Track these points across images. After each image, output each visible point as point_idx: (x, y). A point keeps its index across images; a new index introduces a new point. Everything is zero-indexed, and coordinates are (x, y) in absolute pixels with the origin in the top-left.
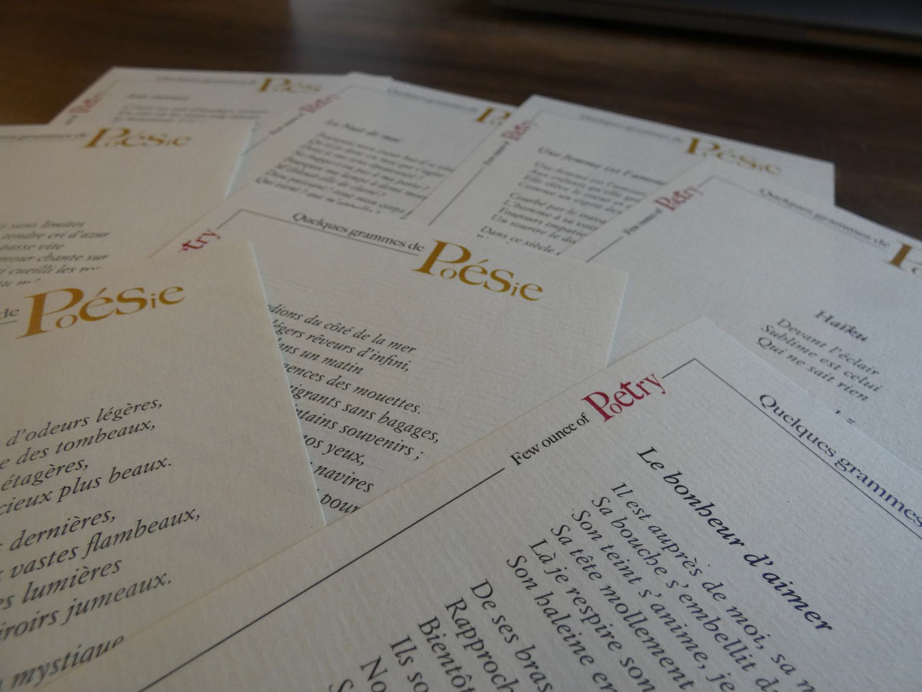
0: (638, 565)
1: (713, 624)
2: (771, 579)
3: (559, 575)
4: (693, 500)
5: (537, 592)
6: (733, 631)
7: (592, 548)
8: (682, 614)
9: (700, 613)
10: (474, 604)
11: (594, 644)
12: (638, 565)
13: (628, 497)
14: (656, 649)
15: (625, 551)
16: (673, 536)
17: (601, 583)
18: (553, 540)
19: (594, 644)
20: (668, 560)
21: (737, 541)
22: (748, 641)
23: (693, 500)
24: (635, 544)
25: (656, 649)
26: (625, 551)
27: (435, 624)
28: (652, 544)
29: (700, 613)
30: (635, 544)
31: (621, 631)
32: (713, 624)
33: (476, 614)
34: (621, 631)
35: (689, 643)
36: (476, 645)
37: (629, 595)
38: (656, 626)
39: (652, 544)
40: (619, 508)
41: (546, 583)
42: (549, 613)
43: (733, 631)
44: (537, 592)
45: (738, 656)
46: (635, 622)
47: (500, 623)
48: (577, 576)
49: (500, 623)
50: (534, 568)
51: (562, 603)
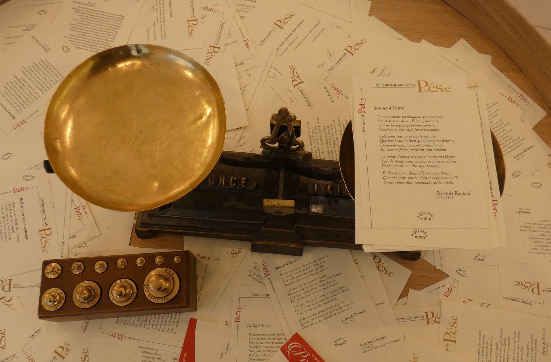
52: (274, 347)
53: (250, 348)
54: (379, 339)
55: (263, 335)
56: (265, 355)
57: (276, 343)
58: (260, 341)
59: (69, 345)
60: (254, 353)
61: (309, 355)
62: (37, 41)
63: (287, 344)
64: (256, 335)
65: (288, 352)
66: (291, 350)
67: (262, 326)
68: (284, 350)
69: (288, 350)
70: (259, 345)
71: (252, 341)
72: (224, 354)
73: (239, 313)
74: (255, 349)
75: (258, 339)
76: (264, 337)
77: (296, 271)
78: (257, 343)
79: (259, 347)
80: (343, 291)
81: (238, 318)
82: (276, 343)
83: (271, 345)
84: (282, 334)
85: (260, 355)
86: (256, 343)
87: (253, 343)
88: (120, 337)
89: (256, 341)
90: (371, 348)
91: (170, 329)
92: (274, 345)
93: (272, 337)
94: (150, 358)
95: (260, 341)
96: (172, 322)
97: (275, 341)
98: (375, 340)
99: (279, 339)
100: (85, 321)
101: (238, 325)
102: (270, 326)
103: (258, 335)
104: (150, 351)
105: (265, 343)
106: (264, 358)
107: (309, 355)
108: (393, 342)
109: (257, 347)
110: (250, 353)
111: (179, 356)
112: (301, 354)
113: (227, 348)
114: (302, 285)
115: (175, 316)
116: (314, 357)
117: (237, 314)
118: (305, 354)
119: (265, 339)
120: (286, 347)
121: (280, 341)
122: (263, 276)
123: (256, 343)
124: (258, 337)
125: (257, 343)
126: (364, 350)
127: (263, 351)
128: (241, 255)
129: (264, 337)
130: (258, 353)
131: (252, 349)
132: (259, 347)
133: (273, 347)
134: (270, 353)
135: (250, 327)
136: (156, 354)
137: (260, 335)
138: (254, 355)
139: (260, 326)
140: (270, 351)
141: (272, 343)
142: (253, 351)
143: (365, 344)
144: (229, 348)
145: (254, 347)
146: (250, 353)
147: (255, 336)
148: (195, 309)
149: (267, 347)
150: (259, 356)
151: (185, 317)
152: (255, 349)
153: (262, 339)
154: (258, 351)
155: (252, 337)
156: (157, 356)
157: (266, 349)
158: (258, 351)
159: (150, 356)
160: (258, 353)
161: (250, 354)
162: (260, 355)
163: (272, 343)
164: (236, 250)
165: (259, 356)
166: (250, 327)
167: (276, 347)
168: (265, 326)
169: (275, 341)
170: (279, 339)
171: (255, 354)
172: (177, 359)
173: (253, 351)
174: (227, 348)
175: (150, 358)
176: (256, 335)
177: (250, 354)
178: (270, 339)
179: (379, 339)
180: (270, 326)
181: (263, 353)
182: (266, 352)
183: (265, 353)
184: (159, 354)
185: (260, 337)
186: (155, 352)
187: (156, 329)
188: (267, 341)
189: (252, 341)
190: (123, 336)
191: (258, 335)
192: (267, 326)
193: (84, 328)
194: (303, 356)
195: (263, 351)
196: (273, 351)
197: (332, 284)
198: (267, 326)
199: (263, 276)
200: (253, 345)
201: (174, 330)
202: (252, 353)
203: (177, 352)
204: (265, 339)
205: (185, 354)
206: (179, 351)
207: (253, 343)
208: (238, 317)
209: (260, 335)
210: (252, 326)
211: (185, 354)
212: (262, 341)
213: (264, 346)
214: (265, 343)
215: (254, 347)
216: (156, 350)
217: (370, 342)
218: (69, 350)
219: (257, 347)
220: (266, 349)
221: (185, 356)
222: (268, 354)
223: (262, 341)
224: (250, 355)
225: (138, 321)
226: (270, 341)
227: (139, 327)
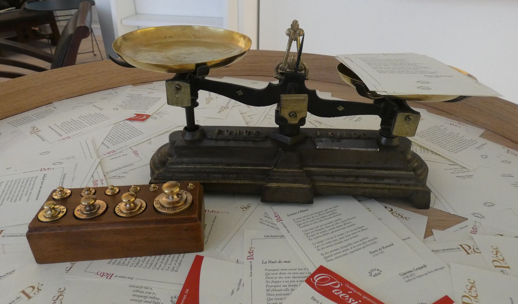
52: (297, 281)
53: (267, 283)
54: (420, 268)
56: (287, 290)
57: (298, 277)
59: (43, 285)
61: (342, 285)
62: (96, 107)
63: (313, 275)
64: (274, 270)
65: (315, 284)
66: (318, 281)
67: (280, 262)
68: (309, 281)
69: (314, 281)
70: (278, 280)
71: (269, 276)
72: (235, 291)
73: (252, 251)
74: (274, 284)
75: (277, 274)
77: (309, 217)
79: (278, 282)
80: (363, 230)
81: (250, 256)
82: (298, 277)
84: (304, 269)
85: (281, 290)
86: (274, 278)
88: (109, 276)
89: (274, 276)
90: (414, 277)
91: (171, 268)
92: (296, 280)
93: (292, 272)
94: (142, 297)
96: (174, 262)
98: (415, 269)
99: (300, 274)
100: (72, 263)
101: (251, 262)
104: (142, 290)
105: (286, 278)
106: (287, 292)
107: (342, 285)
108: (437, 270)
109: (276, 282)
110: (268, 288)
111: (178, 294)
112: (332, 285)
113: (239, 284)
114: (318, 227)
115: (179, 256)
116: (348, 286)
117: (249, 252)
118: (336, 284)
120: (311, 279)
121: (302, 275)
122: (276, 222)
123: (274, 278)
124: (275, 272)
125: (276, 278)
126: (407, 279)
128: (250, 210)
130: (277, 288)
131: (270, 284)
135: (266, 263)
136: (150, 293)
138: (273, 290)
139: (277, 262)
141: (294, 277)
142: (271, 286)
143: (405, 274)
144: (241, 285)
147: (272, 272)
148: (201, 250)
149: (288, 281)
151: (189, 258)
152: (274, 284)
153: (280, 274)
154: (277, 286)
155: (269, 272)
156: (151, 295)
157: (287, 284)
158: (277, 286)
159: (142, 294)
160: (277, 288)
162: (281, 290)
163: (294, 277)
164: (246, 206)
166: (266, 263)
167: (299, 281)
168: (283, 262)
169: (295, 275)
170: (300, 274)
171: (275, 289)
172: (176, 297)
173: (271, 286)
174: (239, 284)
175: (142, 297)
176: (274, 270)
178: (290, 273)
179: (420, 268)
183: (287, 288)
184: (154, 293)
185: (279, 272)
186: (149, 290)
187: (154, 268)
188: (287, 275)
189: (269, 276)
190: (113, 275)
193: (68, 269)
194: (334, 287)
196: (295, 286)
197: (349, 225)
199: (276, 222)
200: (271, 280)
201: (175, 269)
202: (270, 288)
203: (177, 290)
205: (187, 290)
206: (180, 288)
208: (250, 255)
210: (267, 263)
211: (187, 290)
214: (286, 278)
216: (151, 289)
217: (410, 272)
218: (41, 290)
219: (276, 282)
220: (287, 284)
221: (187, 292)
222: (290, 288)
225: (134, 261)
226: (292, 275)
227: (135, 266)
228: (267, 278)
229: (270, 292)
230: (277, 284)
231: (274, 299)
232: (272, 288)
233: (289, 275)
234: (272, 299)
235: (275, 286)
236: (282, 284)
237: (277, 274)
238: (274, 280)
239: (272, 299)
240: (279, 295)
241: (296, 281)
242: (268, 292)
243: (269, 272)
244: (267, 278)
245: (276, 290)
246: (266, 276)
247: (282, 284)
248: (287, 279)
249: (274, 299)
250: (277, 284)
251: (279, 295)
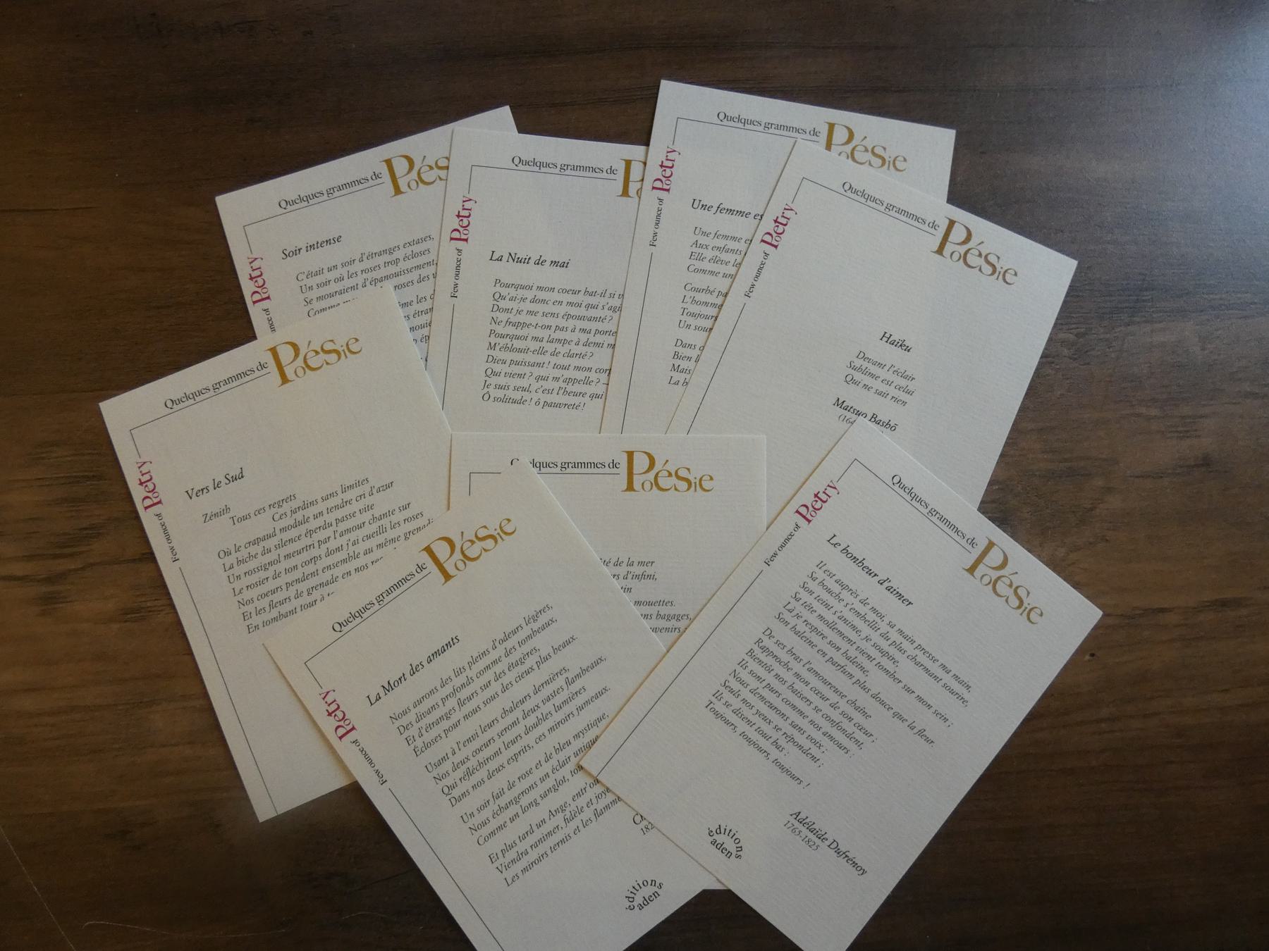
0: (832, 601)
1: (864, 618)
2: (888, 589)
3: (798, 616)
4: (855, 559)
5: (790, 626)
6: (871, 616)
7: (809, 599)
8: (850, 616)
9: (858, 614)
10: (765, 639)
11: (816, 639)
12: (832, 601)
13: (824, 568)
14: (841, 634)
15: (825, 596)
16: (846, 582)
17: (816, 614)
18: (792, 601)
19: (816, 639)
20: (845, 595)
21: (875, 575)
22: (878, 619)
23: (855, 559)
24: (829, 591)
25: (841, 634)
26: (825, 596)
27: (752, 651)
28: (836, 588)
29: (858, 614)
30: (829, 591)
31: (826, 631)
32: (864, 618)
33: (767, 642)
34: (826, 631)
35: (854, 627)
36: (771, 654)
37: (830, 617)
38: (841, 626)
39: (836, 588)
40: (820, 575)
41: (793, 621)
42: (797, 633)
43: (871, 616)
44: (790, 626)
45: (873, 627)
46: (832, 626)
47: (778, 643)
48: (806, 614)
49: (778, 643)
50: (787, 616)
51: (801, 627)
52: (573, 331)
53: (494, 326)
55: (540, 288)
57: (580, 318)
58: (528, 306)
60: (508, 340)
64: (517, 287)
67: (540, 262)
70: (523, 318)
71: (502, 304)
74: (511, 330)
75: (523, 300)
76: (542, 295)
78: (519, 312)
79: (524, 325)
82: (580, 318)
83: (562, 323)
85: (526, 351)
86: (514, 311)
87: (507, 310)
92: (571, 323)
95: (528, 306)
97: (574, 311)
99: (589, 306)
102: (564, 265)
103: (523, 287)
105: (545, 314)
109: (517, 325)
110: (493, 340)
119: (543, 301)
123: (514, 311)
124: (521, 293)
125: (519, 312)
127: (535, 339)
129: (542, 295)
130: (518, 344)
132: (524, 325)
133: (569, 330)
134: (559, 346)
137: (531, 288)
138: (506, 348)
139: (532, 261)
140: (559, 341)
141: (568, 316)
142: (502, 336)
145: (508, 322)
146: (493, 340)
147: (512, 292)
149: (549, 327)
150: (520, 351)
152: (511, 330)
154: (518, 338)
155: (504, 291)
157: (544, 334)
158: (518, 338)
160: (518, 344)
161: (492, 345)
162: (526, 351)
163: (568, 316)
165: (520, 351)
167: (577, 330)
168: (548, 263)
169: (574, 311)
170: (589, 306)
171: (510, 346)
173: (502, 336)
176: (517, 287)
177: (492, 345)
178: (561, 303)
180: (564, 265)
181: (534, 345)
182: (545, 340)
185: (529, 295)
189: (502, 304)
191: (523, 287)
192: (554, 263)
195: (535, 339)
198: (554, 263)
200: (503, 317)
202: (498, 340)
204: (543, 301)
207: (507, 310)
209: (531, 288)
210: (505, 259)
212: (533, 307)
213: (540, 325)
214: (545, 314)
215: (508, 322)
219: (517, 325)
220: (544, 334)
223: (533, 307)
224: (492, 347)
226: (562, 310)
228: (496, 307)
229: (497, 354)
230: (519, 332)
231: (503, 374)
232: (503, 342)
233: (556, 309)
234: (495, 374)
235: (512, 337)
236: (533, 332)
237: (523, 300)
238: (513, 319)
239: (495, 374)
240: (517, 363)
241: (569, 330)
242: (491, 352)
243: (504, 291)
244: (496, 307)
245: (512, 350)
246: (495, 302)
247: (533, 332)
248: (549, 321)
249: (503, 374)
250: (519, 332)
251: (517, 363)
